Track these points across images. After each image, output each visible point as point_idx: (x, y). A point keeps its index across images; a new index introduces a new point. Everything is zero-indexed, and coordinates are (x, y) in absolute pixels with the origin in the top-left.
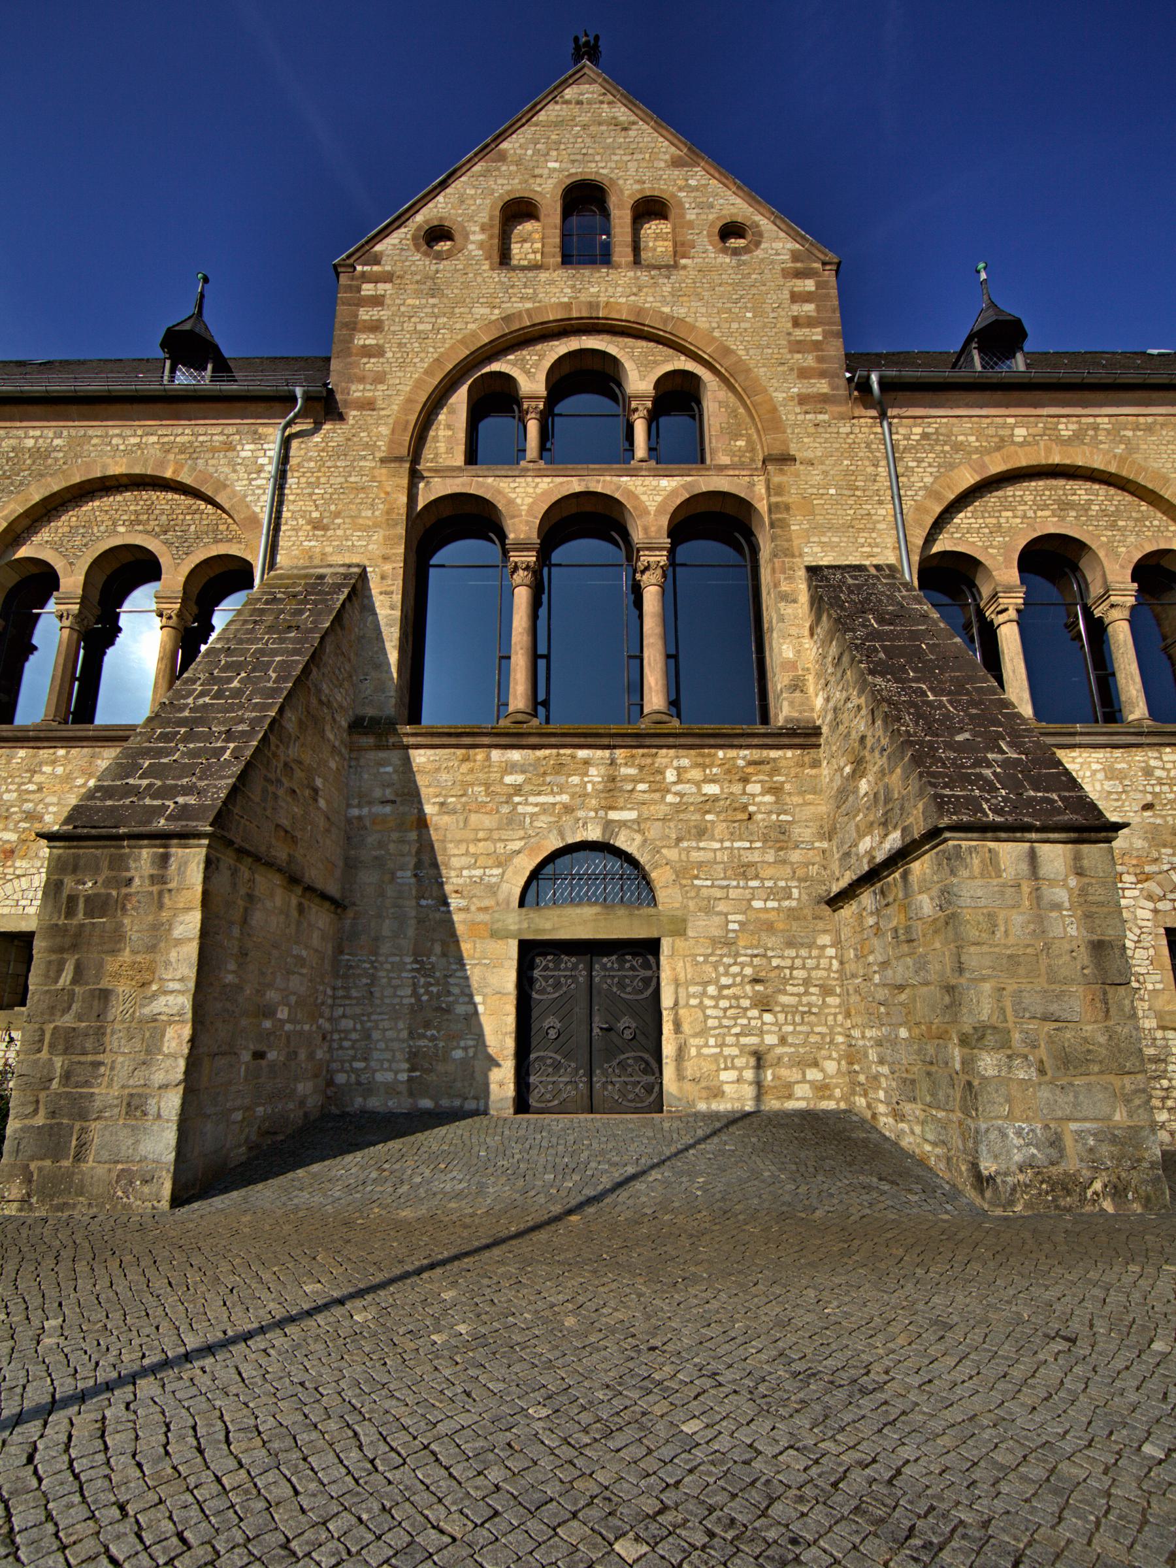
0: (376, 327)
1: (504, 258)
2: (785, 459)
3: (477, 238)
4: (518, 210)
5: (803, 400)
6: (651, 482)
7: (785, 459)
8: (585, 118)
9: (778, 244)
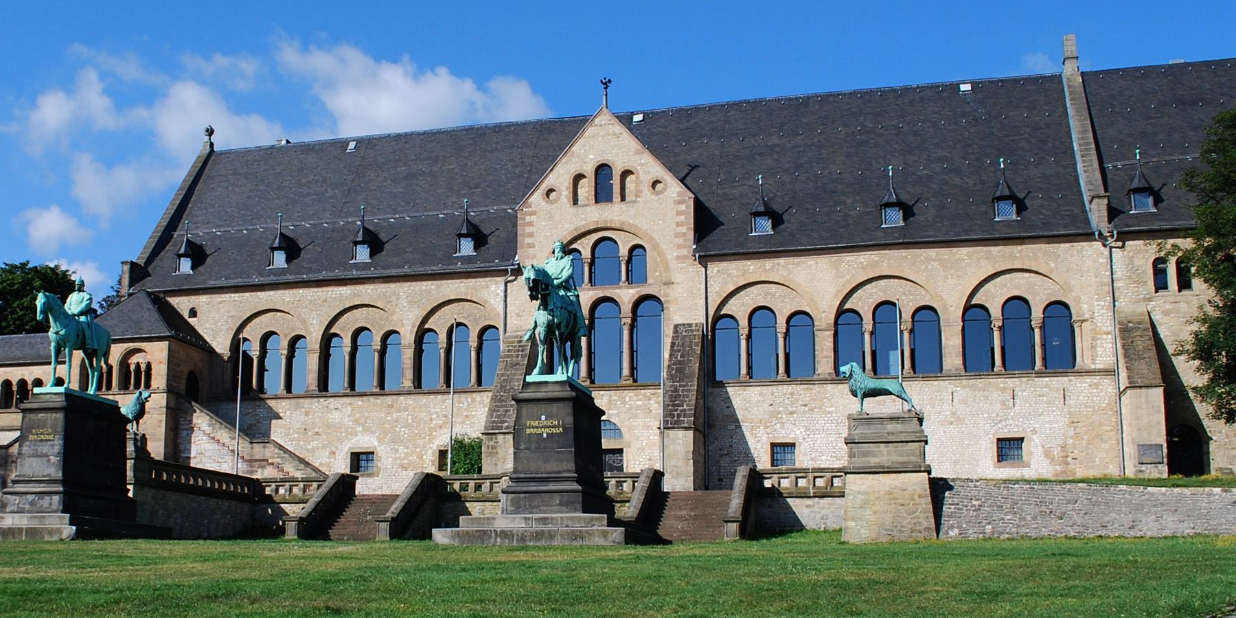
0: (531, 235)
1: (575, 201)
2: (669, 283)
3: (565, 193)
4: (578, 177)
5: (678, 258)
6: (626, 291)
7: (669, 283)
8: (603, 133)
9: (673, 188)
